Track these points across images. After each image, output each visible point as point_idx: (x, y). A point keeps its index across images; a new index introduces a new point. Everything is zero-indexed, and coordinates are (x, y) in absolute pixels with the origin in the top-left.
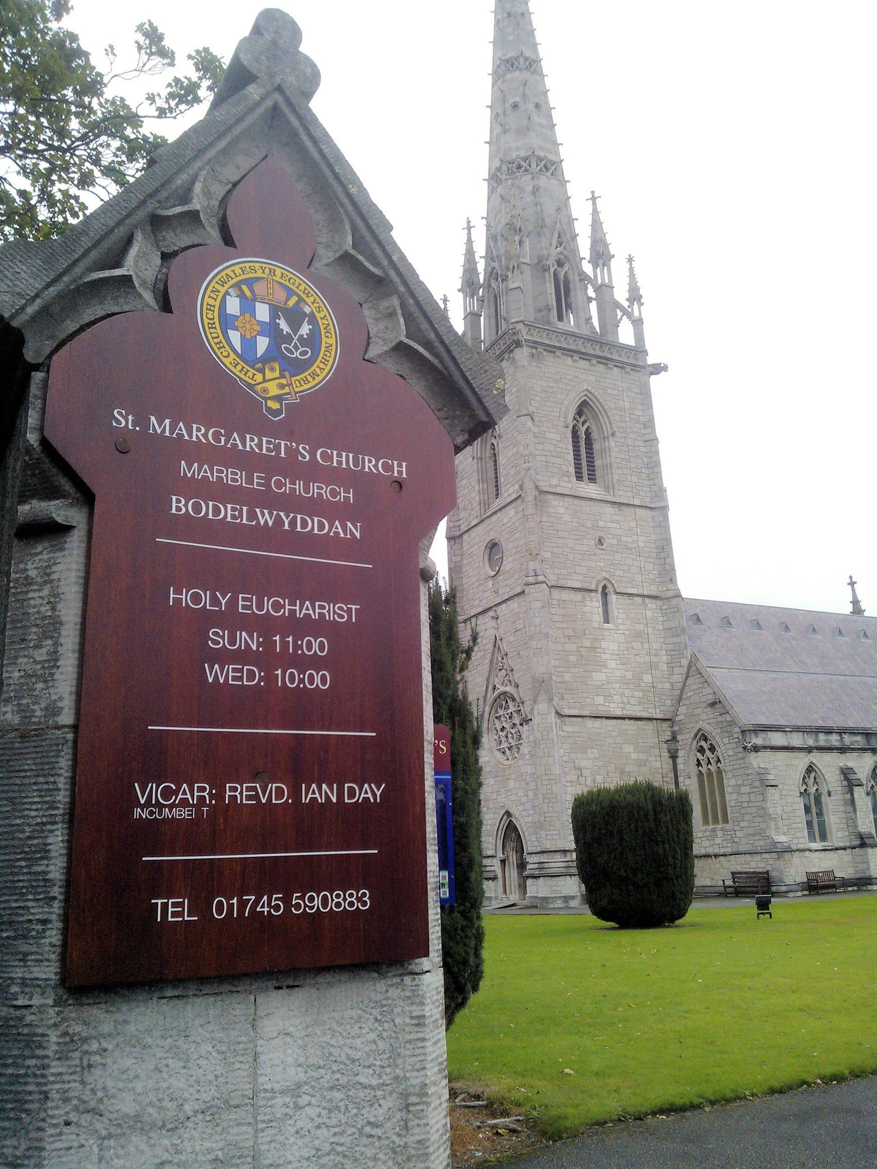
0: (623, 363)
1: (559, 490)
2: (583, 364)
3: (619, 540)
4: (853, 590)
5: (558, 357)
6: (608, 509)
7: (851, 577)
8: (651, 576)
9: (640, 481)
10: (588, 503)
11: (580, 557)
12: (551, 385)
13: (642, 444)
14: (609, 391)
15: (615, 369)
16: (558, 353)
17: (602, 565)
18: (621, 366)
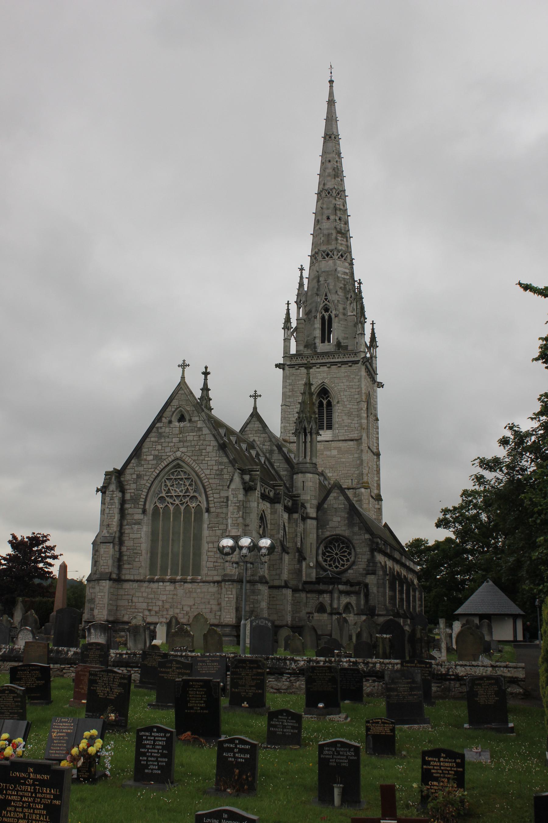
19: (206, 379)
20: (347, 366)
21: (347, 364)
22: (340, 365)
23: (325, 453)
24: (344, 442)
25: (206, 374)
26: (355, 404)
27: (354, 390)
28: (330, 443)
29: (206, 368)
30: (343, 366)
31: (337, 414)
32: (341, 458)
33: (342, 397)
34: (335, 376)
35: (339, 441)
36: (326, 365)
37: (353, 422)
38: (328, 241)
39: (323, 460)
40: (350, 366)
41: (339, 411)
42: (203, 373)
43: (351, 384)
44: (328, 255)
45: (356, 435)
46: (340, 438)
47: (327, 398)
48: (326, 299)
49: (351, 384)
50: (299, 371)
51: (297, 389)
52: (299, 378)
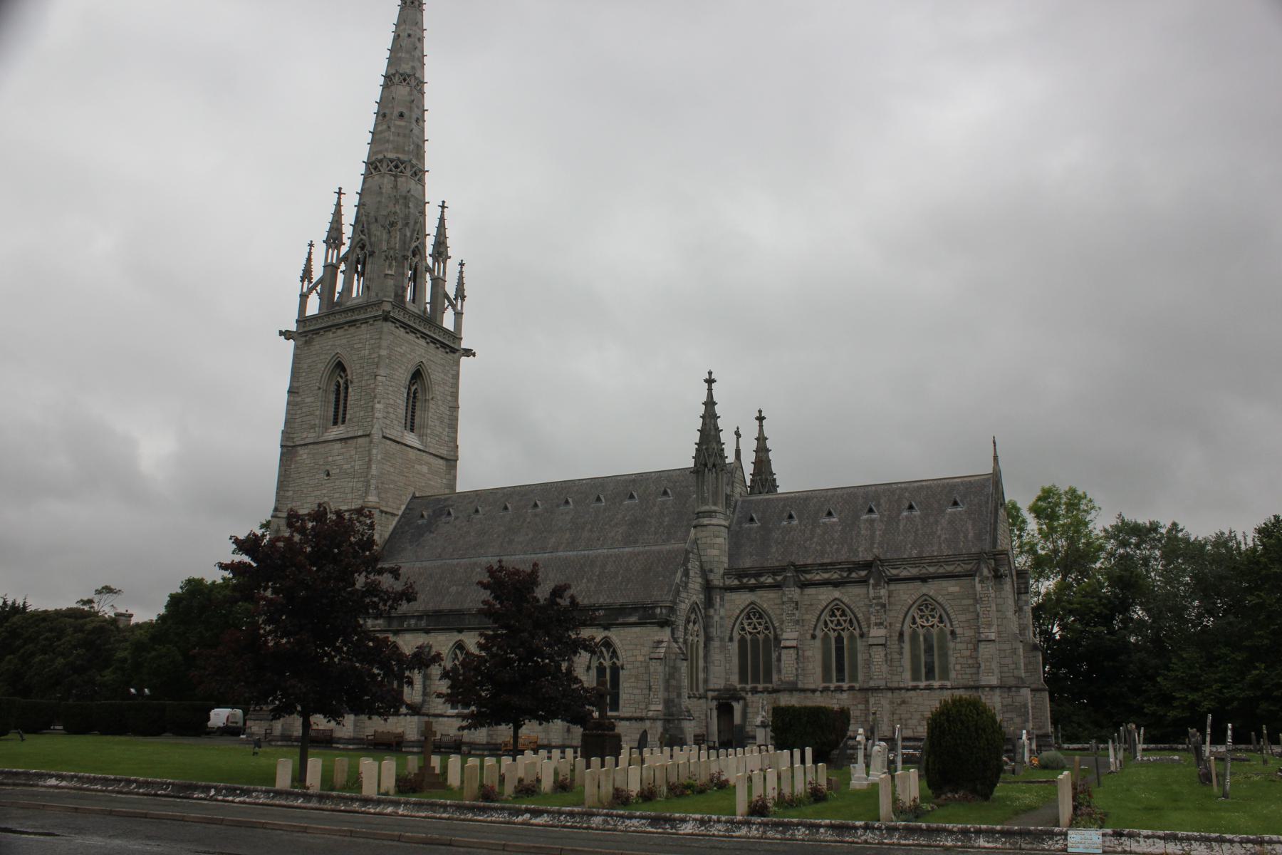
0: (366, 319)
1: (307, 441)
2: (340, 332)
3: (341, 469)
4: (761, 426)
5: (322, 335)
6: (337, 446)
7: (760, 412)
8: (360, 493)
9: (366, 414)
10: (325, 445)
11: (310, 489)
12: (314, 360)
13: (372, 381)
14: (355, 346)
15: (363, 326)
16: (322, 333)
17: (324, 492)
18: (365, 321)
19: (710, 390)
20: (443, 350)
21: (445, 348)
22: (438, 346)
23: (417, 466)
24: (435, 457)
25: (710, 381)
26: (448, 408)
27: (447, 388)
28: (422, 453)
29: (710, 373)
30: (440, 349)
31: (430, 414)
32: (429, 479)
33: (437, 393)
34: (432, 359)
35: (431, 454)
36: (426, 339)
37: (444, 433)
38: (417, 154)
39: (413, 477)
40: (447, 353)
41: (433, 411)
42: (706, 381)
43: (445, 377)
44: (416, 174)
45: (445, 452)
46: (432, 451)
47: (414, 384)
48: (418, 239)
49: (445, 377)
50: (398, 331)
51: (393, 358)
52: (398, 342)
